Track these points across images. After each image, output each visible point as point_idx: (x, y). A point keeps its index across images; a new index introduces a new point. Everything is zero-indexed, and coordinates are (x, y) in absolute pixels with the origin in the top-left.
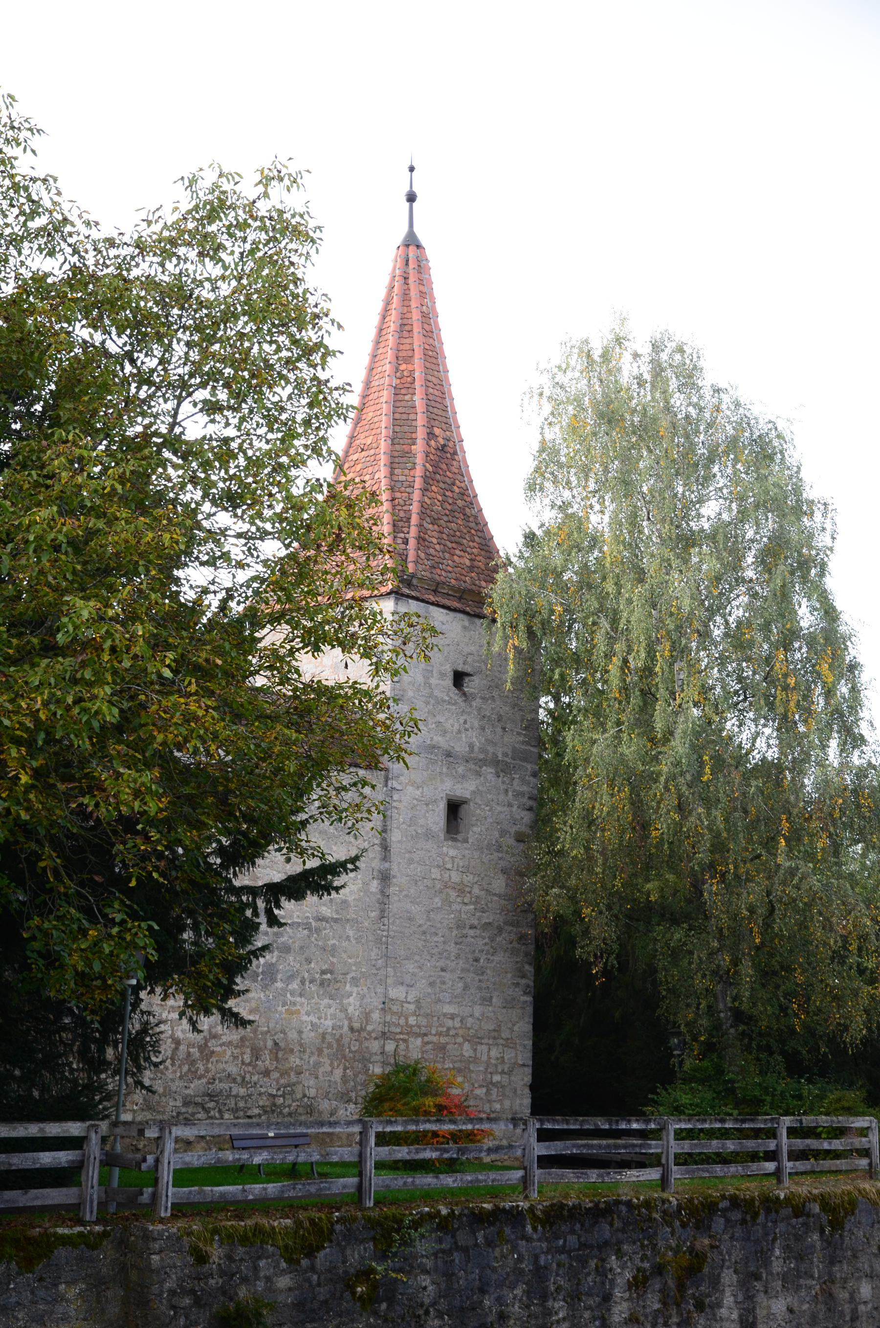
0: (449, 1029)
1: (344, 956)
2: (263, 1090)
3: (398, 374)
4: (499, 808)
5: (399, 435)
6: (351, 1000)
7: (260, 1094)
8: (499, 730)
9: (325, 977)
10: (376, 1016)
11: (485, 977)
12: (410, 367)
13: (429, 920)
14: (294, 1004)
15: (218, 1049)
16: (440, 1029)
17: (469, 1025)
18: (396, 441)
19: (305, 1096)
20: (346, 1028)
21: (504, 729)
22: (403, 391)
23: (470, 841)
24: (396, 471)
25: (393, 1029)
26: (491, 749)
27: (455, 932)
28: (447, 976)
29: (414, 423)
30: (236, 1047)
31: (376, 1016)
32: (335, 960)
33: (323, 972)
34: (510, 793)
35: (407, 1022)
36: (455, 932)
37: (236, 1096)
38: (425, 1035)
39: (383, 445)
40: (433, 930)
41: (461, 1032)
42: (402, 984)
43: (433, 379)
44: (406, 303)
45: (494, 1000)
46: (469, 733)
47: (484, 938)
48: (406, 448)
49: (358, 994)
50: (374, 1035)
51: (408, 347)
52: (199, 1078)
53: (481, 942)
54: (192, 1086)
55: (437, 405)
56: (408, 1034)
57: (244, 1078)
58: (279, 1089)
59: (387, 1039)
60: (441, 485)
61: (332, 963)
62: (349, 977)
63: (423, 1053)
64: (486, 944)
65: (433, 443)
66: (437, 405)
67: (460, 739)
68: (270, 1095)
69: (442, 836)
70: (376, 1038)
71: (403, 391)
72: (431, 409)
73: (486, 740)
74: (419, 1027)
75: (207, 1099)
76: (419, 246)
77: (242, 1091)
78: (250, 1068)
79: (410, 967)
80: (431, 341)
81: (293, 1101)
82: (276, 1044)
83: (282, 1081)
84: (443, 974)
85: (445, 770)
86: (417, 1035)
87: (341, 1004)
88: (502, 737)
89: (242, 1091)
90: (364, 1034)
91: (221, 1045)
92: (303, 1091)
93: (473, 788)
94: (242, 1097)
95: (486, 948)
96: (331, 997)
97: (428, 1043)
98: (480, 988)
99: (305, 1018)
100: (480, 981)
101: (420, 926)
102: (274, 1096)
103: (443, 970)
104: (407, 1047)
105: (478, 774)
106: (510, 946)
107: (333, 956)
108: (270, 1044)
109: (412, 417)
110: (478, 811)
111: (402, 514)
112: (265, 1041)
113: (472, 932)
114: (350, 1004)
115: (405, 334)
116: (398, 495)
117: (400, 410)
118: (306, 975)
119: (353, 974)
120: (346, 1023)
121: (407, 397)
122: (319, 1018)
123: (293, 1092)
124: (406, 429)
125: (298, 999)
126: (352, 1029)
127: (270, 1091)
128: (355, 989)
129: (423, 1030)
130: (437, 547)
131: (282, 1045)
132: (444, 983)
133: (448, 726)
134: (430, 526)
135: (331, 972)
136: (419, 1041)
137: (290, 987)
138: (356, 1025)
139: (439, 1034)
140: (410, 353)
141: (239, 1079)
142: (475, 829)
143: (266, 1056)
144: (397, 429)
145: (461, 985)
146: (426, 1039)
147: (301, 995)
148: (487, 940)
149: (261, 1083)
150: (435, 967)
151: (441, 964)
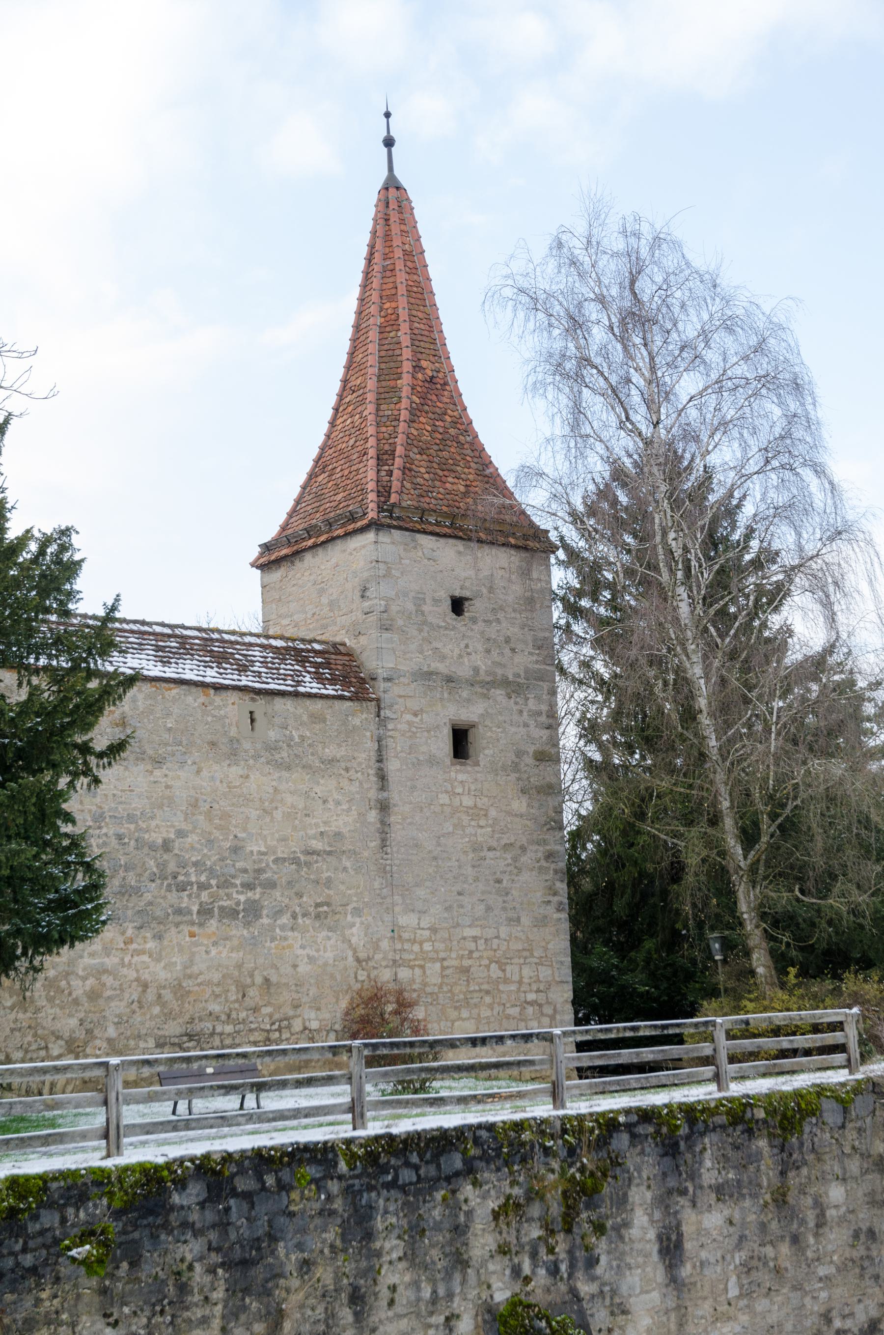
3: (383, 313)
5: (385, 372)
12: (394, 305)
18: (382, 378)
22: (388, 329)
24: (382, 407)
29: (399, 358)
39: (371, 384)
43: (419, 314)
44: (388, 244)
48: (392, 383)
51: (391, 285)
55: (424, 339)
60: (430, 415)
65: (420, 376)
66: (424, 339)
71: (388, 329)
72: (417, 343)
76: (398, 188)
80: (415, 277)
109: (398, 352)
111: (387, 447)
115: (388, 274)
116: (384, 429)
117: (386, 347)
121: (392, 334)
124: (392, 365)
130: (426, 476)
134: (418, 457)
140: (393, 291)
144: (383, 366)
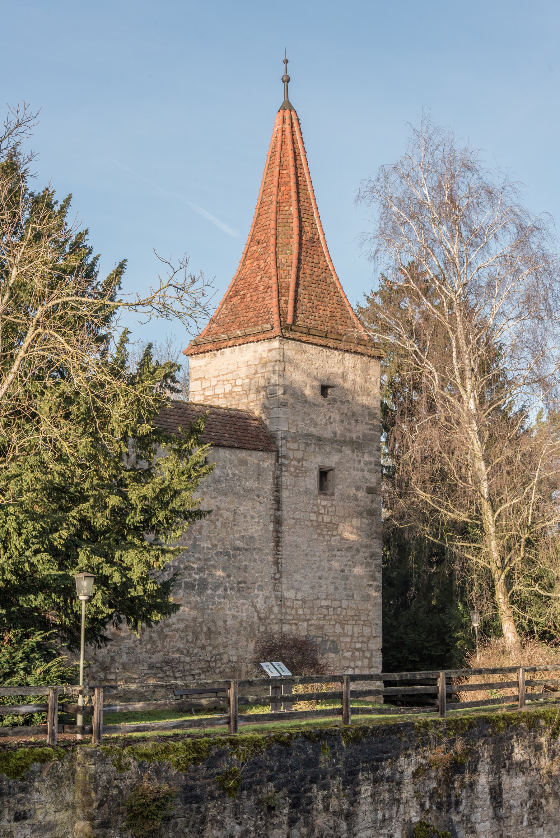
0: (325, 616)
1: (253, 572)
2: (201, 658)
4: (355, 473)
6: (259, 599)
7: (200, 660)
8: (353, 422)
9: (240, 585)
10: (276, 609)
11: (349, 582)
13: (309, 546)
14: (220, 603)
15: (170, 633)
16: (319, 616)
17: (339, 613)
19: (230, 661)
20: (256, 618)
21: (356, 421)
23: (336, 495)
25: (288, 617)
26: (348, 435)
27: (327, 554)
28: (322, 582)
30: (182, 632)
31: (276, 609)
32: (247, 575)
33: (239, 583)
34: (362, 463)
35: (297, 613)
36: (327, 554)
37: (184, 662)
38: (309, 620)
40: (312, 553)
41: (333, 618)
42: (293, 588)
45: (355, 596)
46: (333, 425)
47: (347, 557)
49: (263, 595)
50: (275, 621)
52: (159, 652)
53: (345, 559)
54: (154, 656)
56: (298, 620)
57: (188, 651)
58: (212, 657)
59: (284, 623)
61: (245, 577)
62: (257, 585)
63: (308, 631)
64: (349, 560)
67: (327, 429)
68: (206, 661)
69: (316, 492)
70: (276, 623)
73: (345, 429)
74: (305, 615)
75: (164, 664)
77: (188, 659)
78: (192, 645)
79: (298, 577)
81: (222, 664)
82: (209, 629)
83: (214, 652)
84: (320, 581)
85: (317, 449)
86: (304, 620)
87: (252, 602)
88: (356, 426)
89: (188, 659)
90: (268, 621)
91: (172, 631)
92: (229, 658)
93: (337, 460)
94: (188, 663)
95: (350, 563)
96: (245, 598)
97: (311, 625)
98: (345, 589)
99: (228, 612)
100: (345, 584)
101: (303, 551)
102: (209, 662)
103: (320, 578)
104: (298, 628)
105: (340, 451)
106: (365, 561)
107: (246, 572)
108: (205, 629)
110: (341, 475)
112: (201, 627)
113: (339, 553)
114: (258, 602)
118: (228, 585)
119: (259, 583)
120: (256, 614)
122: (238, 612)
123: (221, 659)
125: (223, 600)
126: (260, 618)
127: (206, 658)
128: (261, 593)
129: (308, 617)
131: (213, 629)
132: (321, 586)
133: (318, 421)
135: (245, 582)
136: (306, 623)
137: (217, 593)
138: (263, 616)
139: (319, 619)
141: (185, 652)
142: (339, 487)
143: (202, 637)
145: (332, 587)
146: (310, 623)
147: (224, 598)
148: (349, 558)
149: (200, 654)
150: (315, 576)
151: (319, 574)
